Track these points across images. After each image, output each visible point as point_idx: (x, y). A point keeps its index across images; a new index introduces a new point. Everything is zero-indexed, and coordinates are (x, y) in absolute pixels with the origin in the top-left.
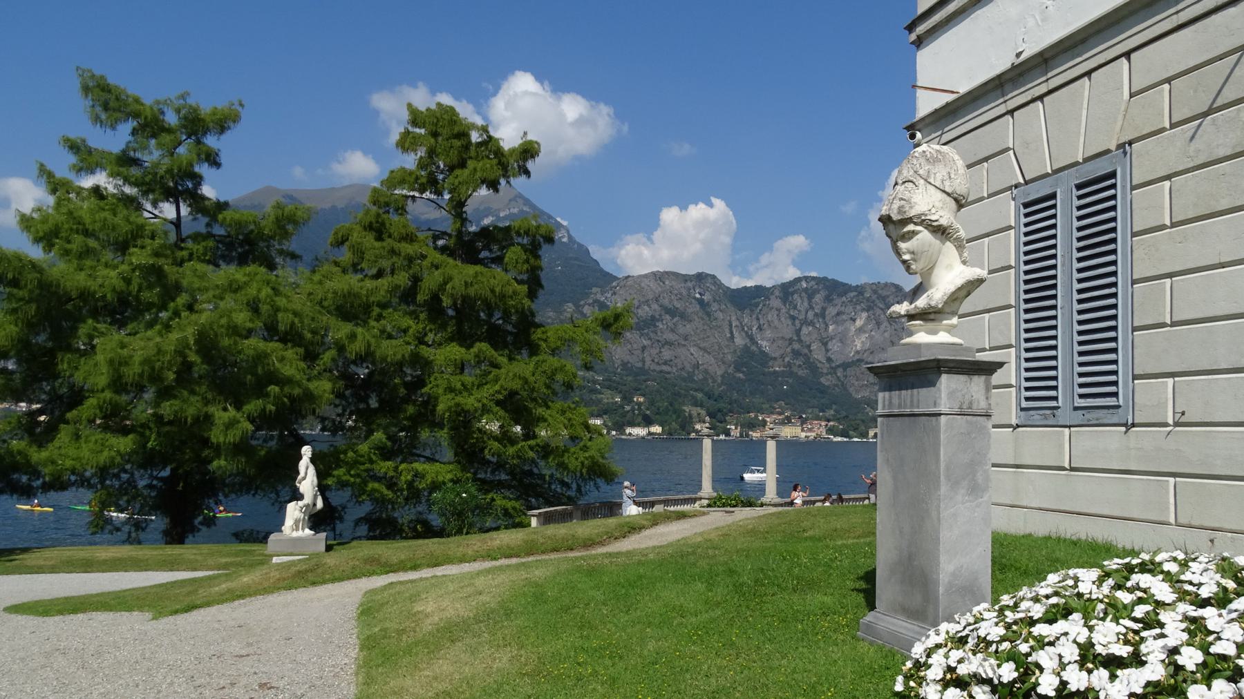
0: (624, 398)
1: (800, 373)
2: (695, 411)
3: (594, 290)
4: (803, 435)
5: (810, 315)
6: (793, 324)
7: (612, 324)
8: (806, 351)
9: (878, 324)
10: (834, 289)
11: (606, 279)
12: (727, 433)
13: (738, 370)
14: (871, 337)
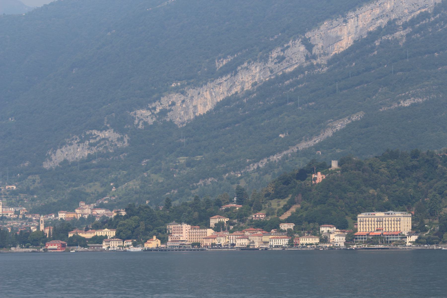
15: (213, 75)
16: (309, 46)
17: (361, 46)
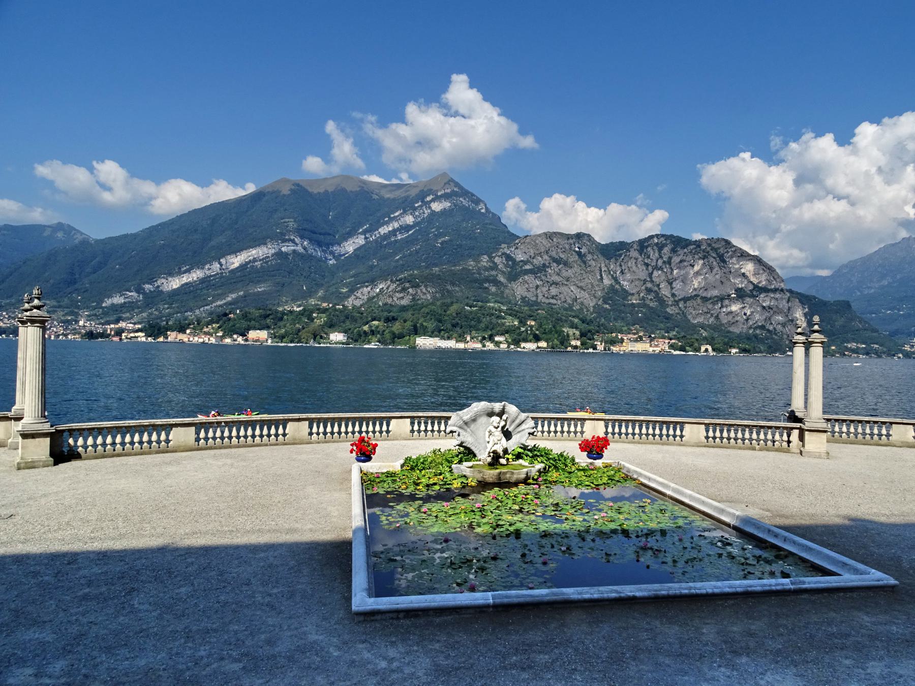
0: (520, 322)
1: (651, 304)
2: (571, 331)
3: (503, 246)
4: (651, 349)
5: (660, 262)
6: (647, 269)
7: (515, 271)
8: (656, 288)
9: (711, 269)
10: (678, 243)
11: (512, 238)
12: (595, 348)
13: (605, 302)
14: (706, 279)
15: (180, 273)
16: (221, 265)
17: (243, 267)
